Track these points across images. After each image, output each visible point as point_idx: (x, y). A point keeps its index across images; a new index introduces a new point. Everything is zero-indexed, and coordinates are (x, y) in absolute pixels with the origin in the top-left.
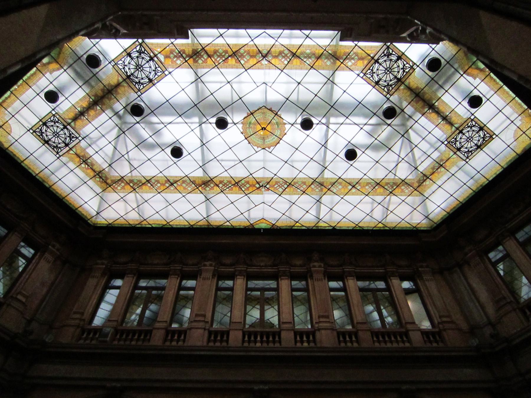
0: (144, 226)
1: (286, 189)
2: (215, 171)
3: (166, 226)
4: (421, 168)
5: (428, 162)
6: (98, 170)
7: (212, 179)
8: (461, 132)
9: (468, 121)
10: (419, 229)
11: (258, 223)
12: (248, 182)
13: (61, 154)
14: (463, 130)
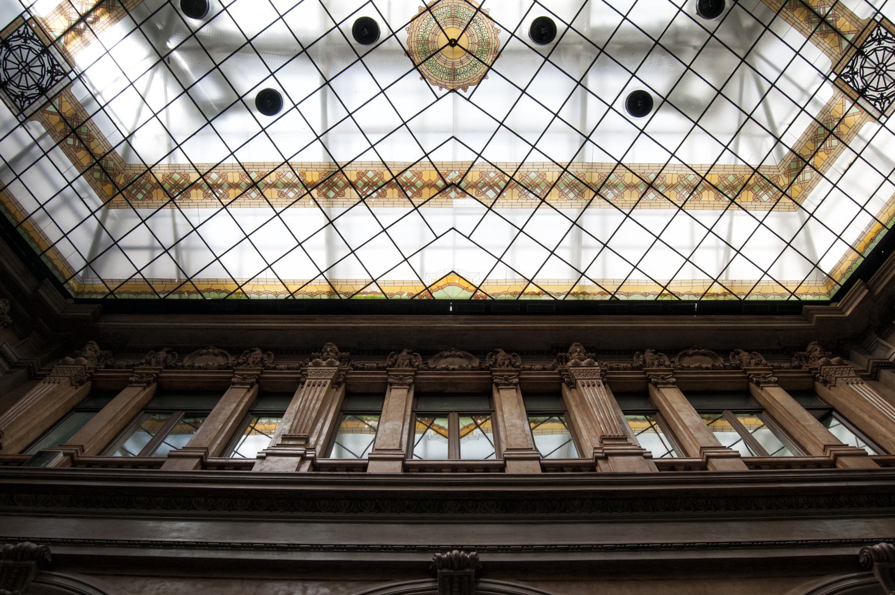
0: (185, 296)
1: (502, 191)
2: (347, 149)
3: (234, 297)
5: (803, 124)
6: (99, 151)
7: (340, 169)
9: (871, 27)
10: (803, 298)
11: (440, 284)
13: (28, 112)
14: (862, 47)
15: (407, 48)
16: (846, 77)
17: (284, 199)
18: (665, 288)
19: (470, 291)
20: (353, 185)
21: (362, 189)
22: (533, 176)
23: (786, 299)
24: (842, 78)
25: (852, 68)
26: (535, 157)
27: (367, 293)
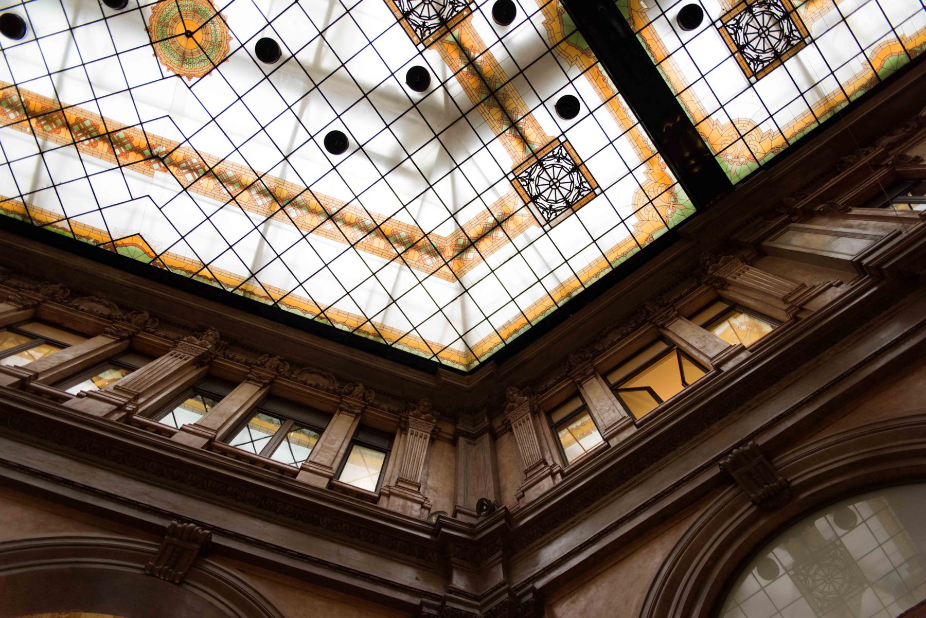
1: (199, 178)
2: (73, 94)
4: (463, 218)
5: (477, 208)
7: (62, 109)
8: (540, 162)
10: (444, 362)
12: (130, 139)
15: (148, 25)
16: (523, 180)
17: (4, 118)
18: (322, 312)
19: (151, 257)
20: (69, 127)
21: (76, 134)
22: (230, 174)
23: (428, 357)
24: (519, 179)
25: (530, 174)
26: (235, 158)
27: (57, 227)
